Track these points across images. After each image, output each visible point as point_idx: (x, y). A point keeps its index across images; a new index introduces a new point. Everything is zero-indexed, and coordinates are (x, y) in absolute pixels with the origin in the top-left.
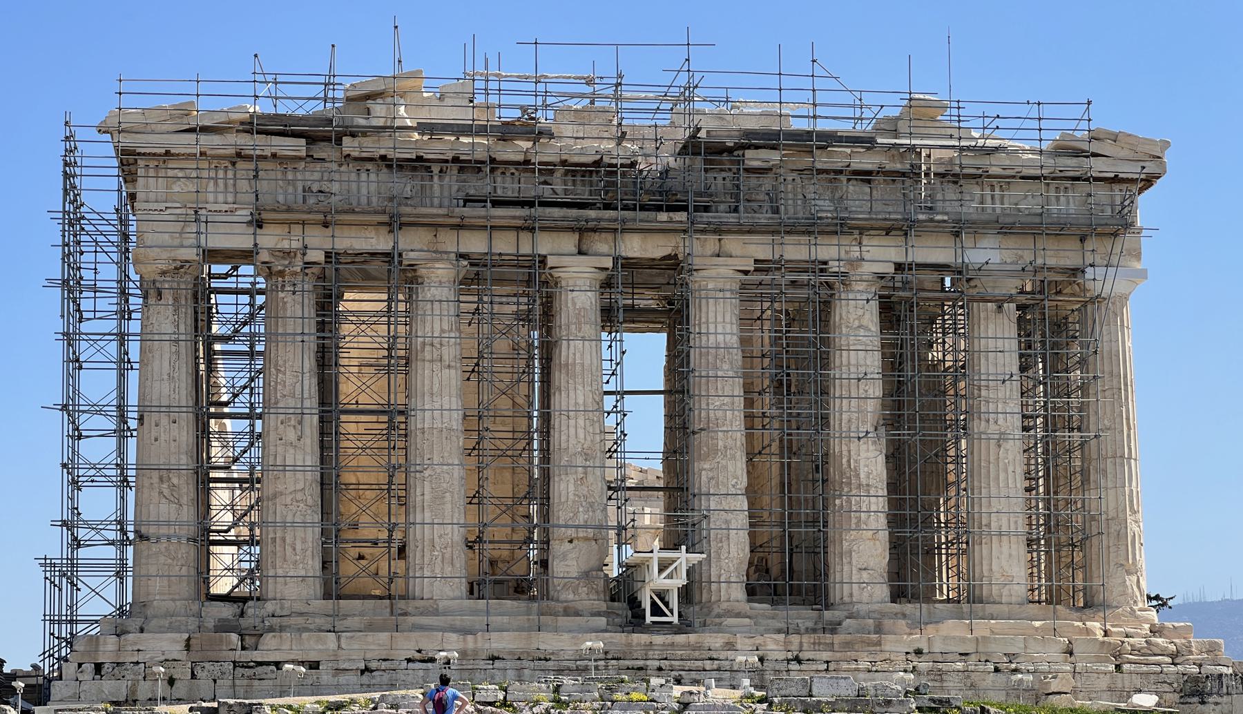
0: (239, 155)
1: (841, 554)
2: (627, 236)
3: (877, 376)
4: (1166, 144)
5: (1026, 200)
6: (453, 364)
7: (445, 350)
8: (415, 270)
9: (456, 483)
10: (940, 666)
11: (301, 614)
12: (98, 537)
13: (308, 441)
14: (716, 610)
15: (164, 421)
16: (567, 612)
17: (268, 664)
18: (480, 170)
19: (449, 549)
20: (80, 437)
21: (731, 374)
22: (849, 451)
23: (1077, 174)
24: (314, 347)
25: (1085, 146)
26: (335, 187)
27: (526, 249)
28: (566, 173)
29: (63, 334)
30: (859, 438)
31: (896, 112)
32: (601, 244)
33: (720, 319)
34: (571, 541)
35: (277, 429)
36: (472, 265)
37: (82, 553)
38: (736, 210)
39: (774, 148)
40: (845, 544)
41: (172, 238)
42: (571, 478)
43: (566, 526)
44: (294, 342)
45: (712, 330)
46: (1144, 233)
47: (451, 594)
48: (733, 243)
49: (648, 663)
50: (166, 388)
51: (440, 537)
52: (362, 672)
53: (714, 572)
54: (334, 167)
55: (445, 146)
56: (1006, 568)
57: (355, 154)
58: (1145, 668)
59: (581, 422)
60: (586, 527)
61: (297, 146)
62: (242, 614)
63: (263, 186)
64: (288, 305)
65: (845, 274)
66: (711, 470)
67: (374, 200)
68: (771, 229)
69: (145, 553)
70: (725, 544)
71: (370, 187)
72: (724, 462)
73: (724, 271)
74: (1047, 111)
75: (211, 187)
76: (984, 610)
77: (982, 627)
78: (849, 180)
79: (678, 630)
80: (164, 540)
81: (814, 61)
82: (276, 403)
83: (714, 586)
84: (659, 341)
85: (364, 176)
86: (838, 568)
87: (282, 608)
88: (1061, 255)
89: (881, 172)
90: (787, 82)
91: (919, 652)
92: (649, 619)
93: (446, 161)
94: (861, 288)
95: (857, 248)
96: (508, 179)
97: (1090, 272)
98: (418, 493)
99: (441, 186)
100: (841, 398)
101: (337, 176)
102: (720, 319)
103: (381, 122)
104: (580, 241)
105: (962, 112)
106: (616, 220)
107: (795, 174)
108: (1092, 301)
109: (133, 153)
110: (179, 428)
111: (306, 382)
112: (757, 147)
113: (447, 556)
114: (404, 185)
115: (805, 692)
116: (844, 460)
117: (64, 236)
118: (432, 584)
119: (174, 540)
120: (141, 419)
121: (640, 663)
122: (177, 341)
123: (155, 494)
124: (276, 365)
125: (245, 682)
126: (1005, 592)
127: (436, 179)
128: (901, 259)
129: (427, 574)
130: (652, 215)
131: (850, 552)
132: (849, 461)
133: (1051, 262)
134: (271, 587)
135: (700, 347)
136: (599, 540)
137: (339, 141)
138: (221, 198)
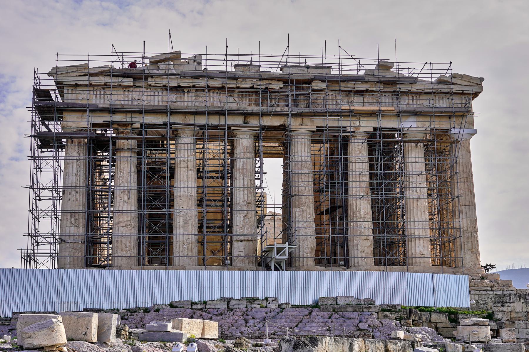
0: (105, 85)
2: (264, 118)
3: (367, 173)
4: (482, 79)
7: (189, 163)
8: (177, 131)
9: (193, 217)
12: (45, 241)
13: (133, 200)
15: (73, 193)
18: (204, 91)
19: (190, 245)
20: (40, 200)
21: (307, 172)
23: (447, 91)
24: (136, 162)
25: (450, 80)
26: (145, 98)
27: (222, 122)
29: (32, 157)
30: (360, 198)
31: (373, 67)
32: (254, 121)
33: (303, 150)
36: (201, 129)
37: (40, 247)
38: (309, 107)
40: (355, 242)
43: (240, 235)
45: (300, 154)
46: (475, 114)
51: (187, 240)
53: (301, 253)
56: (422, 251)
57: (153, 84)
59: (246, 192)
65: (354, 132)
66: (300, 211)
69: (64, 247)
72: (305, 208)
73: (304, 131)
75: (94, 98)
76: (413, 269)
78: (354, 94)
82: (120, 185)
83: (301, 260)
84: (280, 161)
85: (156, 93)
86: (352, 251)
88: (440, 124)
89: (367, 91)
93: (190, 87)
94: (360, 138)
95: (358, 122)
97: (453, 131)
100: (353, 182)
101: (145, 94)
102: (303, 150)
104: (245, 119)
105: (400, 67)
107: (332, 92)
108: (454, 142)
109: (62, 84)
111: (132, 177)
113: (190, 248)
114: (172, 97)
116: (354, 207)
117: (32, 117)
120: (63, 192)
122: (79, 160)
128: (376, 126)
129: (181, 255)
131: (357, 245)
132: (356, 207)
133: (437, 127)
134: (116, 261)
135: (295, 162)
136: (253, 240)
137: (146, 79)
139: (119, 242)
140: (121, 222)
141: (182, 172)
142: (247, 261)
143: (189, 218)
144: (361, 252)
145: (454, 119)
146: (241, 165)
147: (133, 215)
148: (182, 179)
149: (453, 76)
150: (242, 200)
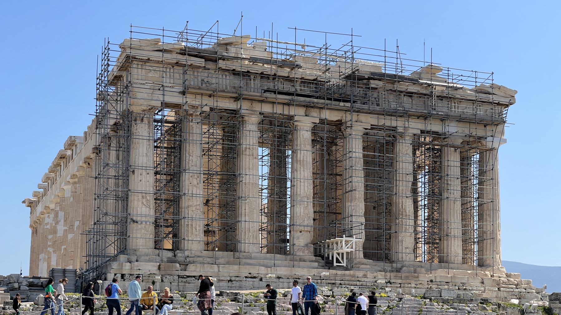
4: (516, 92)
5: (467, 110)
10: (440, 287)
11: (199, 257)
14: (355, 262)
15: (144, 173)
16: (301, 260)
17: (191, 277)
26: (214, 81)
27: (286, 112)
28: (302, 82)
30: (407, 197)
32: (315, 113)
33: (357, 147)
34: (301, 232)
39: (380, 80)
40: (400, 238)
41: (148, 95)
42: (302, 206)
43: (300, 226)
44: (196, 143)
47: (256, 251)
48: (363, 117)
49: (337, 281)
50: (145, 159)
51: (252, 227)
52: (229, 281)
54: (213, 72)
55: (259, 68)
57: (224, 68)
58: (508, 290)
59: (306, 184)
60: (307, 226)
61: (200, 62)
62: (175, 256)
63: (187, 77)
64: (194, 128)
67: (228, 87)
68: (379, 112)
69: (135, 228)
71: (228, 81)
77: (452, 272)
78: (404, 95)
79: (346, 269)
80: (144, 223)
81: (398, 47)
87: (191, 254)
88: (479, 131)
90: (388, 54)
91: (432, 281)
92: (335, 264)
96: (280, 83)
99: (254, 84)
103: (233, 55)
106: (324, 104)
112: (374, 79)
115: (439, 295)
116: (400, 205)
118: (249, 246)
119: (148, 223)
121: (333, 282)
122: (149, 140)
123: (140, 203)
124: (189, 153)
125: (183, 284)
126: (456, 259)
127: (252, 80)
128: (423, 128)
130: (337, 103)
131: (402, 241)
138: (168, 81)
145: (488, 128)
146: (302, 157)
149: (492, 86)
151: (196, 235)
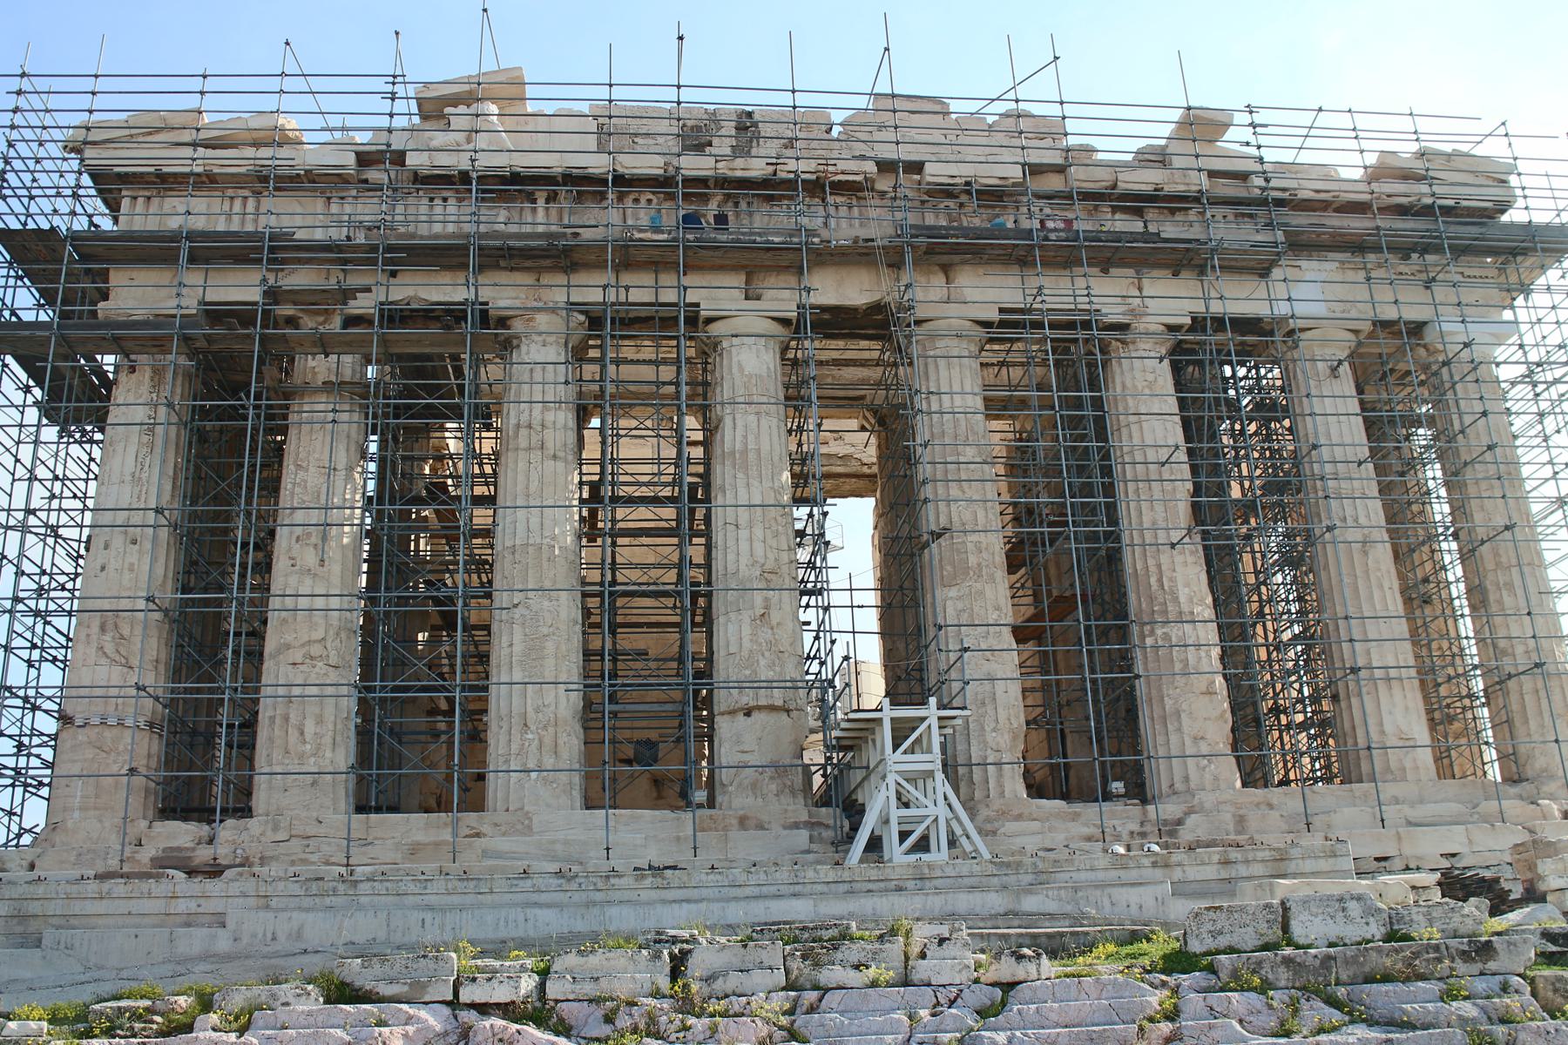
1: (1164, 718)
6: (561, 454)
9: (563, 627)
15: (118, 540)
19: (551, 730)
22: (1159, 566)
30: (1173, 546)
35: (290, 549)
40: (1168, 703)
42: (746, 616)
51: (537, 710)
59: (758, 532)
66: (959, 598)
70: (990, 708)
74: (1362, 122)
83: (977, 773)
98: (505, 644)
110: (140, 551)
113: (548, 741)
116: (1153, 580)
123: (92, 651)
131: (1178, 714)
132: (1160, 580)
139: (278, 721)
140: (288, 647)
141: (521, 465)
142: (773, 787)
143: (545, 630)
144: (1196, 739)
146: (739, 438)
147: (336, 623)
148: (520, 487)
150: (744, 560)
151: (301, 756)
